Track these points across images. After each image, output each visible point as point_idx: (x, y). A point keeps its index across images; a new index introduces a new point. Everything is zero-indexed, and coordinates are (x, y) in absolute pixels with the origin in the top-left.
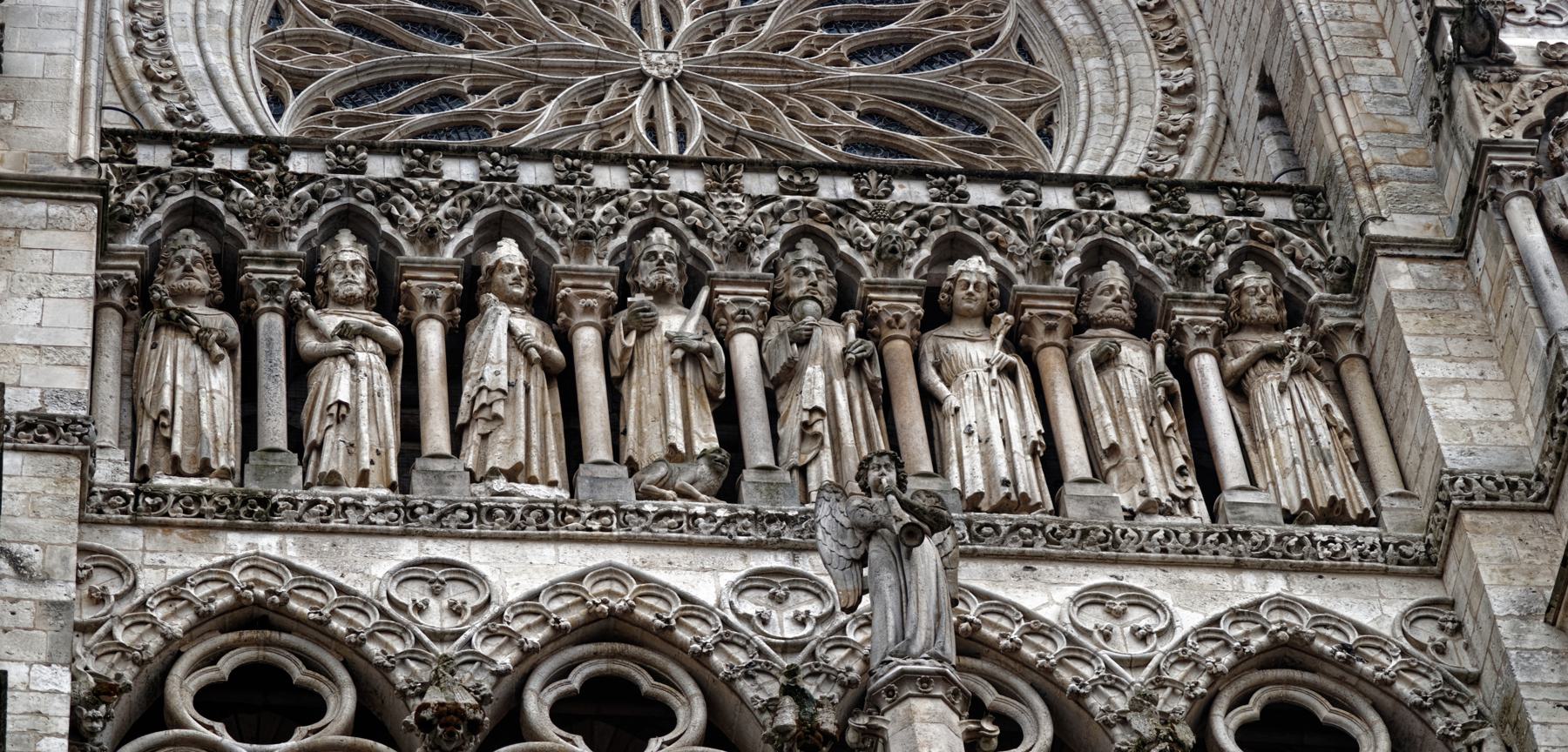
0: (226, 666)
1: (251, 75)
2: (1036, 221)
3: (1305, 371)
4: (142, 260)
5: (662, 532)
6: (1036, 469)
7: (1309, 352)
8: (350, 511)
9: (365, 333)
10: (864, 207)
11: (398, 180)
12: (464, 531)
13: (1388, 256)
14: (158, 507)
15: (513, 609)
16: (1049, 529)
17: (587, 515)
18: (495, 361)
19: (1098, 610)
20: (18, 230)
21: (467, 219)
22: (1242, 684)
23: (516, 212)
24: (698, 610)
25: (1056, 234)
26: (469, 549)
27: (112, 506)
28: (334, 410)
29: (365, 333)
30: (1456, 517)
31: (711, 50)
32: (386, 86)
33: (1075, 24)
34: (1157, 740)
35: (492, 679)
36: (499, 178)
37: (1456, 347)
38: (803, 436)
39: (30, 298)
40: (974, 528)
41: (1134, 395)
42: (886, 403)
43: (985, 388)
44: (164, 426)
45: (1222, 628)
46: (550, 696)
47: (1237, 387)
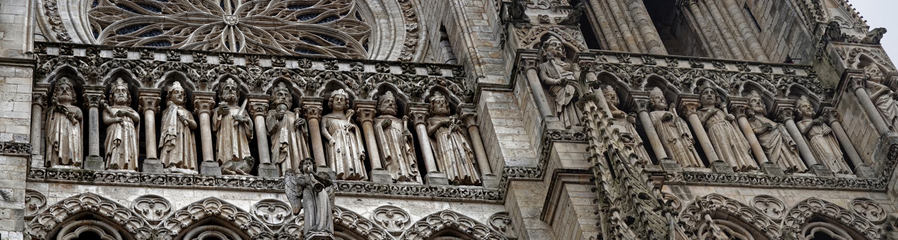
0: (77, 232)
1: (87, 23)
3: (456, 131)
4: (48, 88)
5: (231, 186)
6: (362, 165)
7: (458, 124)
8: (121, 178)
9: (127, 115)
10: (302, 71)
11: (138, 60)
13: (485, 90)
14: (54, 176)
16: (366, 186)
19: (383, 215)
20: (5, 77)
21: (163, 74)
23: (180, 72)
27: (38, 175)
28: (116, 142)
29: (127, 115)
30: (509, 183)
31: (248, 16)
32: (135, 27)
33: (376, 7)
35: (171, 238)
36: (174, 60)
37: (510, 122)
38: (280, 152)
39: (9, 101)
40: (340, 185)
41: (396, 139)
42: (309, 141)
43: (344, 136)
44: (56, 147)
47: (433, 136)
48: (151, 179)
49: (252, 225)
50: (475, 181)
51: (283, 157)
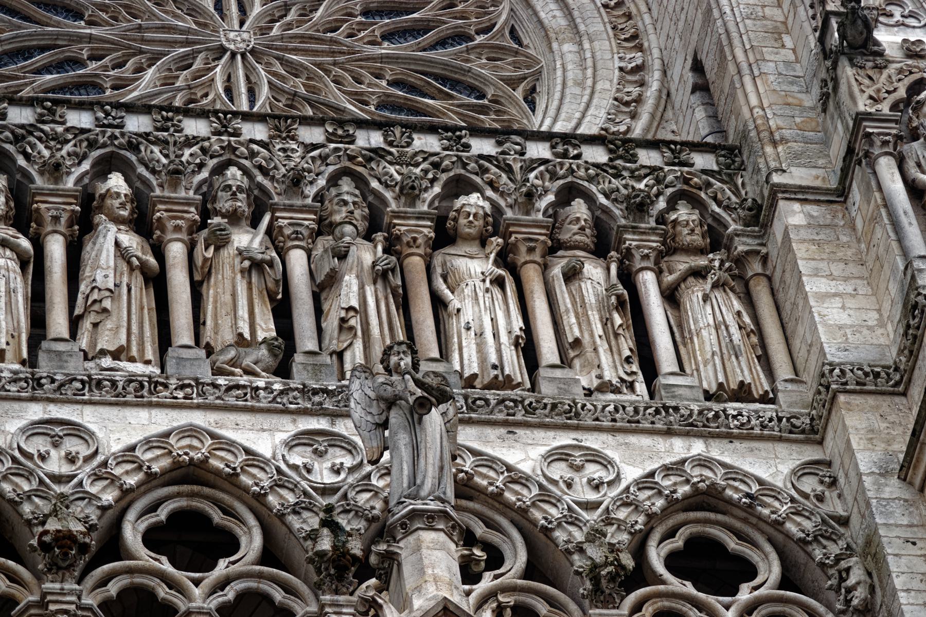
2: (521, 167)
3: (723, 285)
5: (232, 401)
6: (518, 357)
7: (726, 271)
10: (391, 153)
11: (31, 125)
12: (78, 397)
13: (786, 199)
15: (115, 458)
16: (527, 402)
17: (174, 387)
18: (105, 267)
19: (563, 465)
21: (85, 157)
22: (671, 522)
23: (123, 152)
24: (258, 461)
25: (536, 178)
26: (82, 411)
30: (834, 398)
31: (276, 31)
32: (24, 53)
33: (554, 17)
34: (606, 564)
35: (98, 512)
36: (110, 126)
38: (341, 328)
40: (470, 401)
41: (593, 301)
42: (405, 305)
43: (480, 294)
45: (656, 480)
46: (143, 526)
47: (671, 297)
48: (56, 384)
49: (278, 485)
50: (761, 392)
51: (346, 339)
